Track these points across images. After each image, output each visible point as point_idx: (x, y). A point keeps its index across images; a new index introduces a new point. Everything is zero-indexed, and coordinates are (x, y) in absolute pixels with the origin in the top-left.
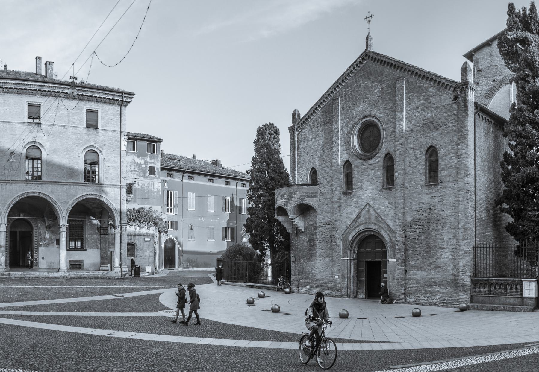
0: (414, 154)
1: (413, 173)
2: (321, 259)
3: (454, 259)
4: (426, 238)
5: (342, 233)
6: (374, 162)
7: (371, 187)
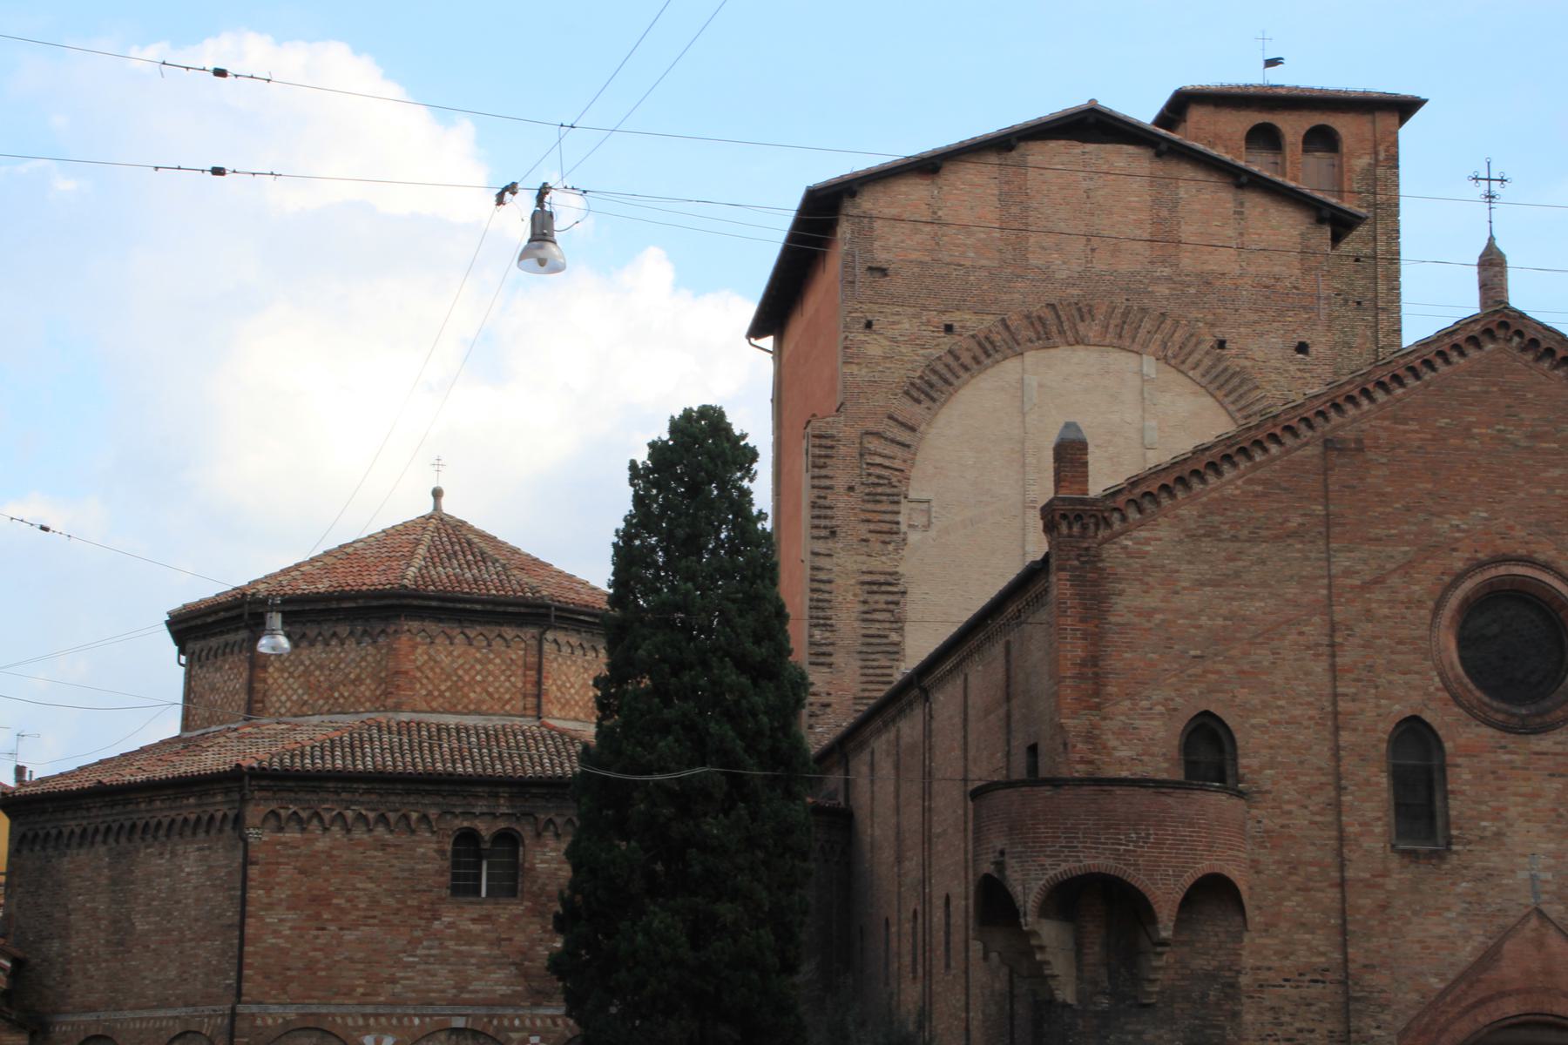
6: (1559, 749)
7: (1552, 846)
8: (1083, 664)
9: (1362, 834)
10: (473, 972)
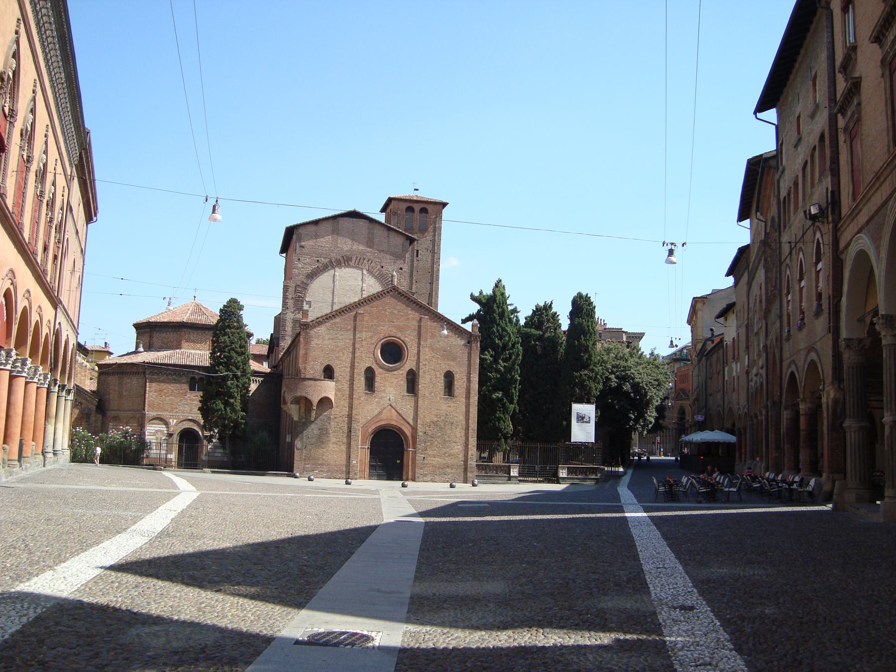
2: (335, 446)
4: (443, 435)
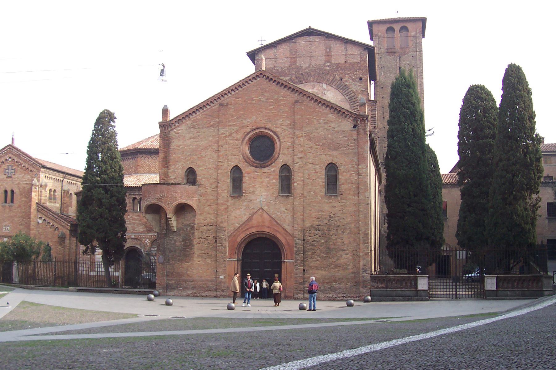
0: (314, 168)
1: (312, 184)
2: (200, 259)
3: (354, 259)
4: (326, 241)
5: (229, 235)
6: (269, 171)
7: (266, 193)
8: (163, 158)
9: (222, 193)
10: (136, 226)
